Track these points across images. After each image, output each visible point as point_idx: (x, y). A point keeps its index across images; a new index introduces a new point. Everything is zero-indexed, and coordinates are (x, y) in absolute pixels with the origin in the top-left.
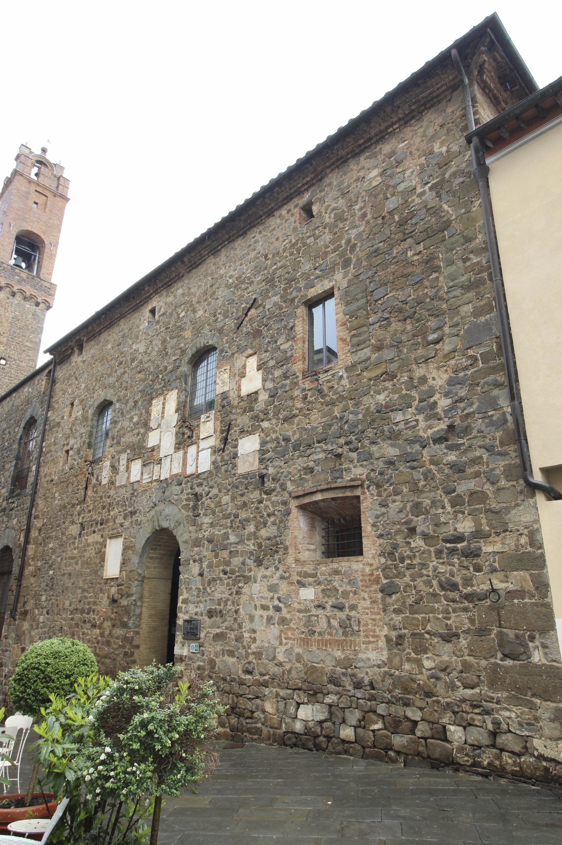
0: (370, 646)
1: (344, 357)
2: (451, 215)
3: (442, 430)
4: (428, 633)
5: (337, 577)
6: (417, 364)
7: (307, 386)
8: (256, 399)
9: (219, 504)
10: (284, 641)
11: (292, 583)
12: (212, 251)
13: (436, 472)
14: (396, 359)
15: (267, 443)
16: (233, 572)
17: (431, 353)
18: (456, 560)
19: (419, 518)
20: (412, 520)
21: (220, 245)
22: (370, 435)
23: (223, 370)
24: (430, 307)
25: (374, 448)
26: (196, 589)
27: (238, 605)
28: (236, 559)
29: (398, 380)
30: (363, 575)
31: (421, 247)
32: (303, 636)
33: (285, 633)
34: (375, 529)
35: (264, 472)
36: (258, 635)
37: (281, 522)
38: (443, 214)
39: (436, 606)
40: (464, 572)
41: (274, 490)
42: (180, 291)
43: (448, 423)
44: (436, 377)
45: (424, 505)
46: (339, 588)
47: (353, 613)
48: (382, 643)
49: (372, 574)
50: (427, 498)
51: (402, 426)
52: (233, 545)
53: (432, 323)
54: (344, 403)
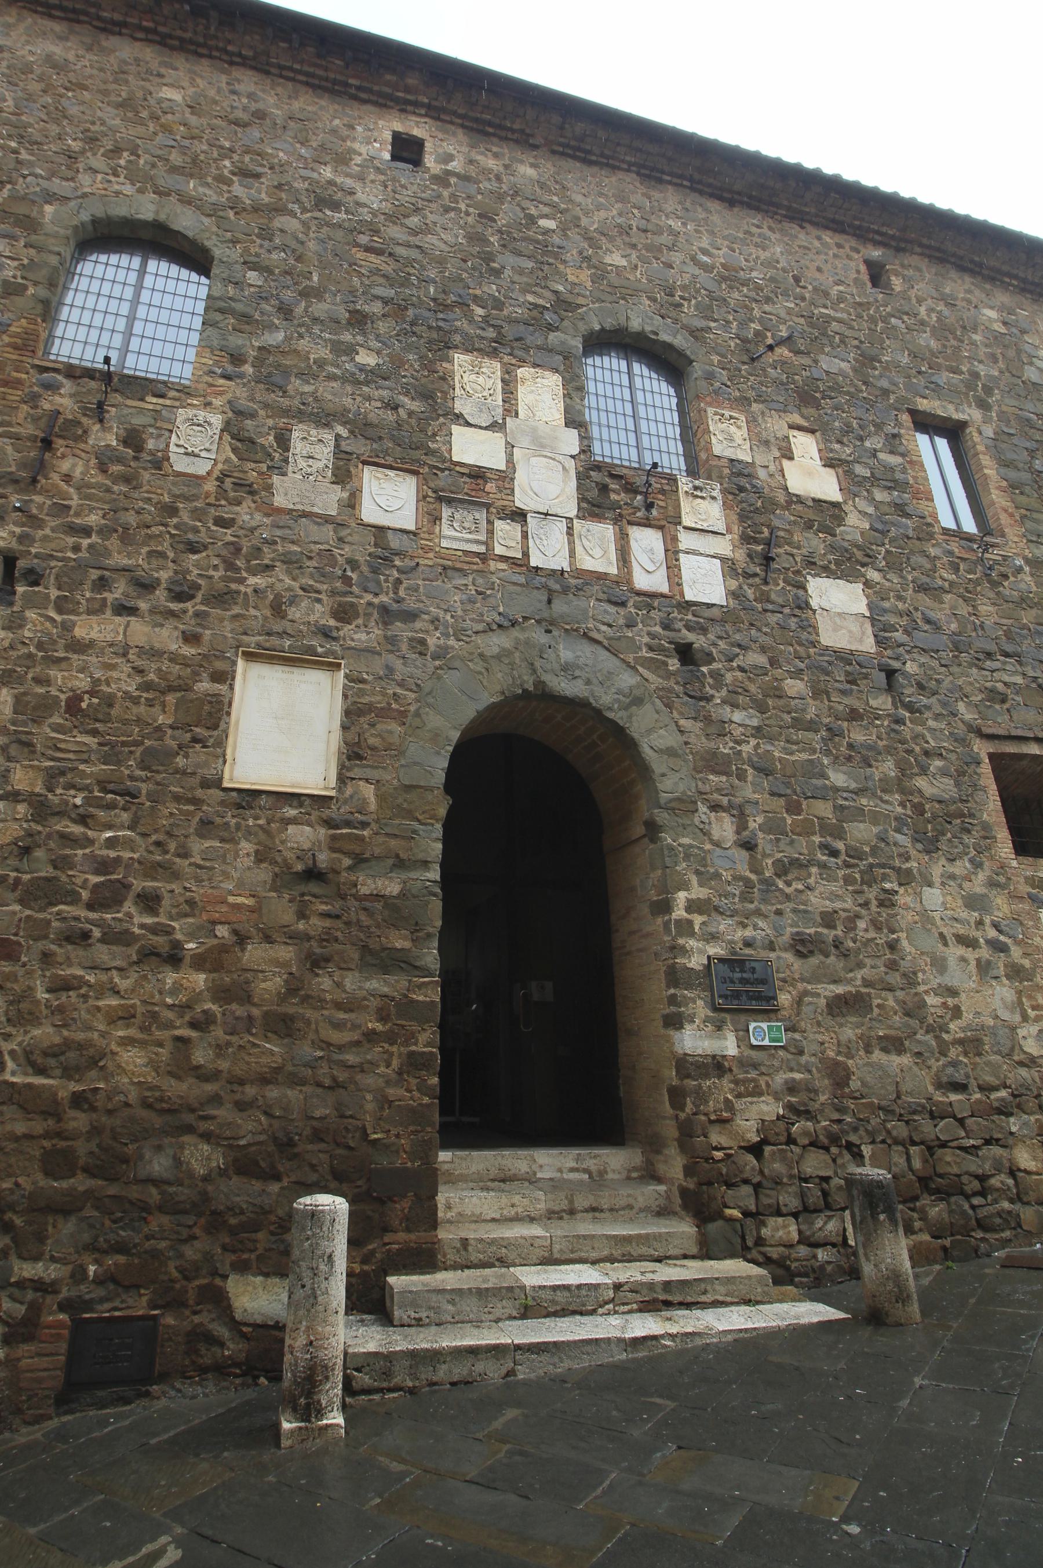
12: (644, 167)
16: (855, 853)
21: (670, 174)
27: (893, 932)
28: (862, 826)
33: (1030, 997)
42: (526, 171)
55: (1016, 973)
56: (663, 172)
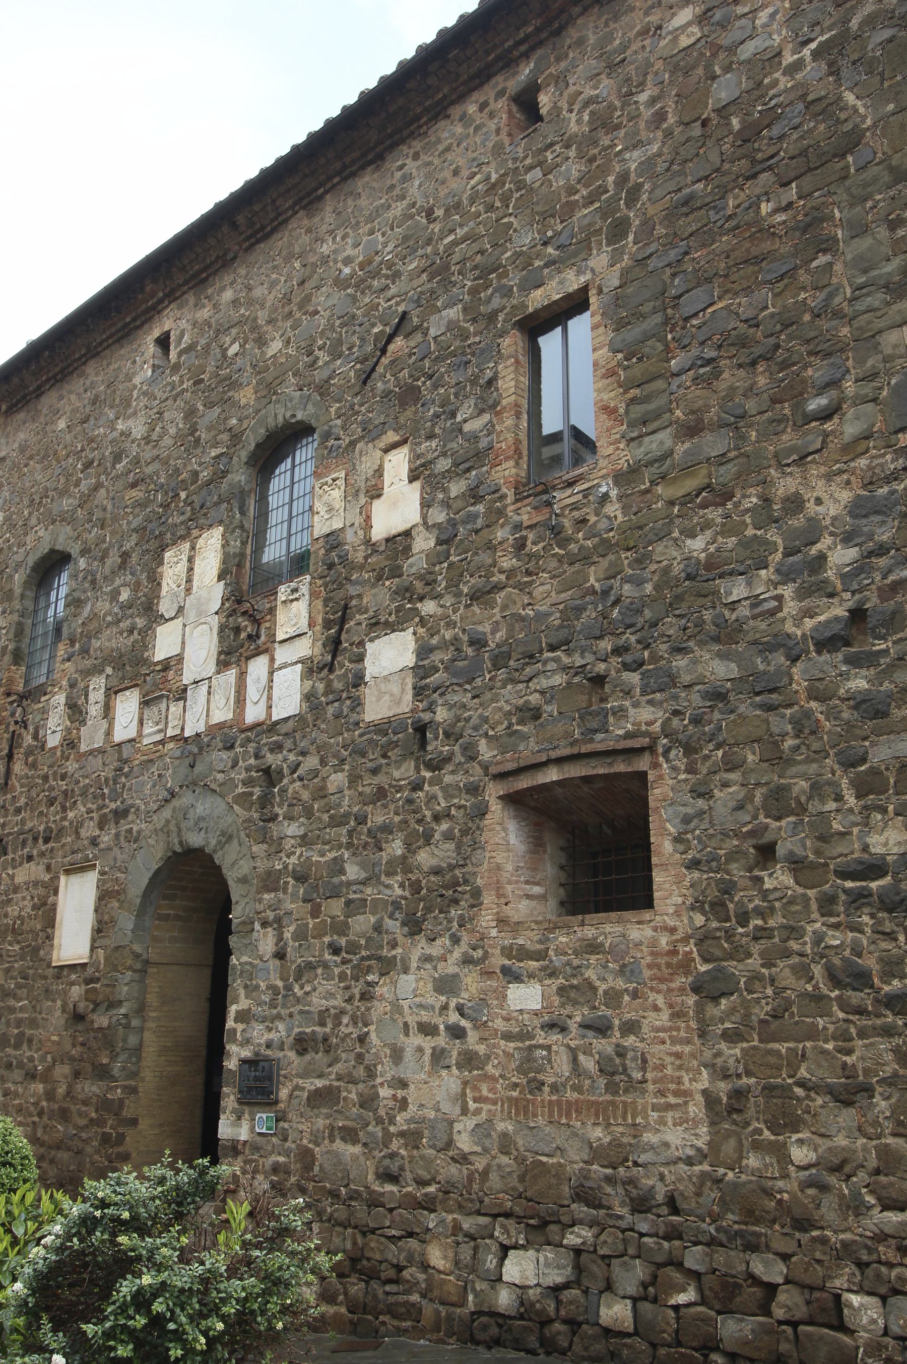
0: (670, 1116)
1: (610, 450)
2: (864, 118)
3: (837, 619)
4: (801, 1084)
5: (593, 959)
6: (781, 466)
7: (525, 517)
8: (407, 550)
9: (321, 793)
10: (472, 1105)
11: (488, 974)
12: (302, 199)
13: (821, 717)
14: (733, 454)
15: (432, 650)
16: (353, 948)
17: (813, 442)
18: (866, 919)
19: (783, 823)
20: (766, 827)
21: (321, 185)
22: (671, 632)
23: (329, 480)
24: (812, 334)
25: (680, 662)
26: (269, 987)
27: (366, 1025)
28: (361, 918)
29: (737, 505)
30: (652, 954)
31: (793, 190)
32: (515, 1094)
33: (475, 1088)
34: (681, 848)
35: (426, 717)
36: (412, 1094)
37: (465, 832)
38: (843, 116)
39: (820, 1022)
40: (884, 945)
41: (448, 759)
42: (228, 295)
43: (850, 604)
44: (825, 497)
45: (796, 790)
46: (598, 983)
47: (631, 1040)
48: (696, 1108)
49: (674, 952)
50: (804, 776)
51: (744, 611)
52: (354, 888)
53: (816, 372)
54: (611, 557)
55: (469, 1060)
56: (316, 189)
